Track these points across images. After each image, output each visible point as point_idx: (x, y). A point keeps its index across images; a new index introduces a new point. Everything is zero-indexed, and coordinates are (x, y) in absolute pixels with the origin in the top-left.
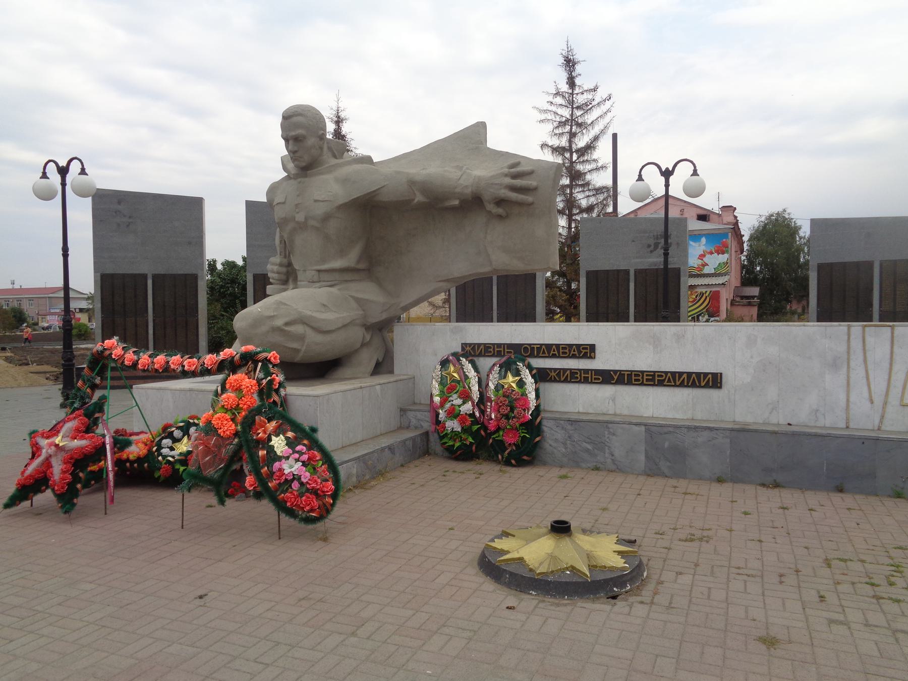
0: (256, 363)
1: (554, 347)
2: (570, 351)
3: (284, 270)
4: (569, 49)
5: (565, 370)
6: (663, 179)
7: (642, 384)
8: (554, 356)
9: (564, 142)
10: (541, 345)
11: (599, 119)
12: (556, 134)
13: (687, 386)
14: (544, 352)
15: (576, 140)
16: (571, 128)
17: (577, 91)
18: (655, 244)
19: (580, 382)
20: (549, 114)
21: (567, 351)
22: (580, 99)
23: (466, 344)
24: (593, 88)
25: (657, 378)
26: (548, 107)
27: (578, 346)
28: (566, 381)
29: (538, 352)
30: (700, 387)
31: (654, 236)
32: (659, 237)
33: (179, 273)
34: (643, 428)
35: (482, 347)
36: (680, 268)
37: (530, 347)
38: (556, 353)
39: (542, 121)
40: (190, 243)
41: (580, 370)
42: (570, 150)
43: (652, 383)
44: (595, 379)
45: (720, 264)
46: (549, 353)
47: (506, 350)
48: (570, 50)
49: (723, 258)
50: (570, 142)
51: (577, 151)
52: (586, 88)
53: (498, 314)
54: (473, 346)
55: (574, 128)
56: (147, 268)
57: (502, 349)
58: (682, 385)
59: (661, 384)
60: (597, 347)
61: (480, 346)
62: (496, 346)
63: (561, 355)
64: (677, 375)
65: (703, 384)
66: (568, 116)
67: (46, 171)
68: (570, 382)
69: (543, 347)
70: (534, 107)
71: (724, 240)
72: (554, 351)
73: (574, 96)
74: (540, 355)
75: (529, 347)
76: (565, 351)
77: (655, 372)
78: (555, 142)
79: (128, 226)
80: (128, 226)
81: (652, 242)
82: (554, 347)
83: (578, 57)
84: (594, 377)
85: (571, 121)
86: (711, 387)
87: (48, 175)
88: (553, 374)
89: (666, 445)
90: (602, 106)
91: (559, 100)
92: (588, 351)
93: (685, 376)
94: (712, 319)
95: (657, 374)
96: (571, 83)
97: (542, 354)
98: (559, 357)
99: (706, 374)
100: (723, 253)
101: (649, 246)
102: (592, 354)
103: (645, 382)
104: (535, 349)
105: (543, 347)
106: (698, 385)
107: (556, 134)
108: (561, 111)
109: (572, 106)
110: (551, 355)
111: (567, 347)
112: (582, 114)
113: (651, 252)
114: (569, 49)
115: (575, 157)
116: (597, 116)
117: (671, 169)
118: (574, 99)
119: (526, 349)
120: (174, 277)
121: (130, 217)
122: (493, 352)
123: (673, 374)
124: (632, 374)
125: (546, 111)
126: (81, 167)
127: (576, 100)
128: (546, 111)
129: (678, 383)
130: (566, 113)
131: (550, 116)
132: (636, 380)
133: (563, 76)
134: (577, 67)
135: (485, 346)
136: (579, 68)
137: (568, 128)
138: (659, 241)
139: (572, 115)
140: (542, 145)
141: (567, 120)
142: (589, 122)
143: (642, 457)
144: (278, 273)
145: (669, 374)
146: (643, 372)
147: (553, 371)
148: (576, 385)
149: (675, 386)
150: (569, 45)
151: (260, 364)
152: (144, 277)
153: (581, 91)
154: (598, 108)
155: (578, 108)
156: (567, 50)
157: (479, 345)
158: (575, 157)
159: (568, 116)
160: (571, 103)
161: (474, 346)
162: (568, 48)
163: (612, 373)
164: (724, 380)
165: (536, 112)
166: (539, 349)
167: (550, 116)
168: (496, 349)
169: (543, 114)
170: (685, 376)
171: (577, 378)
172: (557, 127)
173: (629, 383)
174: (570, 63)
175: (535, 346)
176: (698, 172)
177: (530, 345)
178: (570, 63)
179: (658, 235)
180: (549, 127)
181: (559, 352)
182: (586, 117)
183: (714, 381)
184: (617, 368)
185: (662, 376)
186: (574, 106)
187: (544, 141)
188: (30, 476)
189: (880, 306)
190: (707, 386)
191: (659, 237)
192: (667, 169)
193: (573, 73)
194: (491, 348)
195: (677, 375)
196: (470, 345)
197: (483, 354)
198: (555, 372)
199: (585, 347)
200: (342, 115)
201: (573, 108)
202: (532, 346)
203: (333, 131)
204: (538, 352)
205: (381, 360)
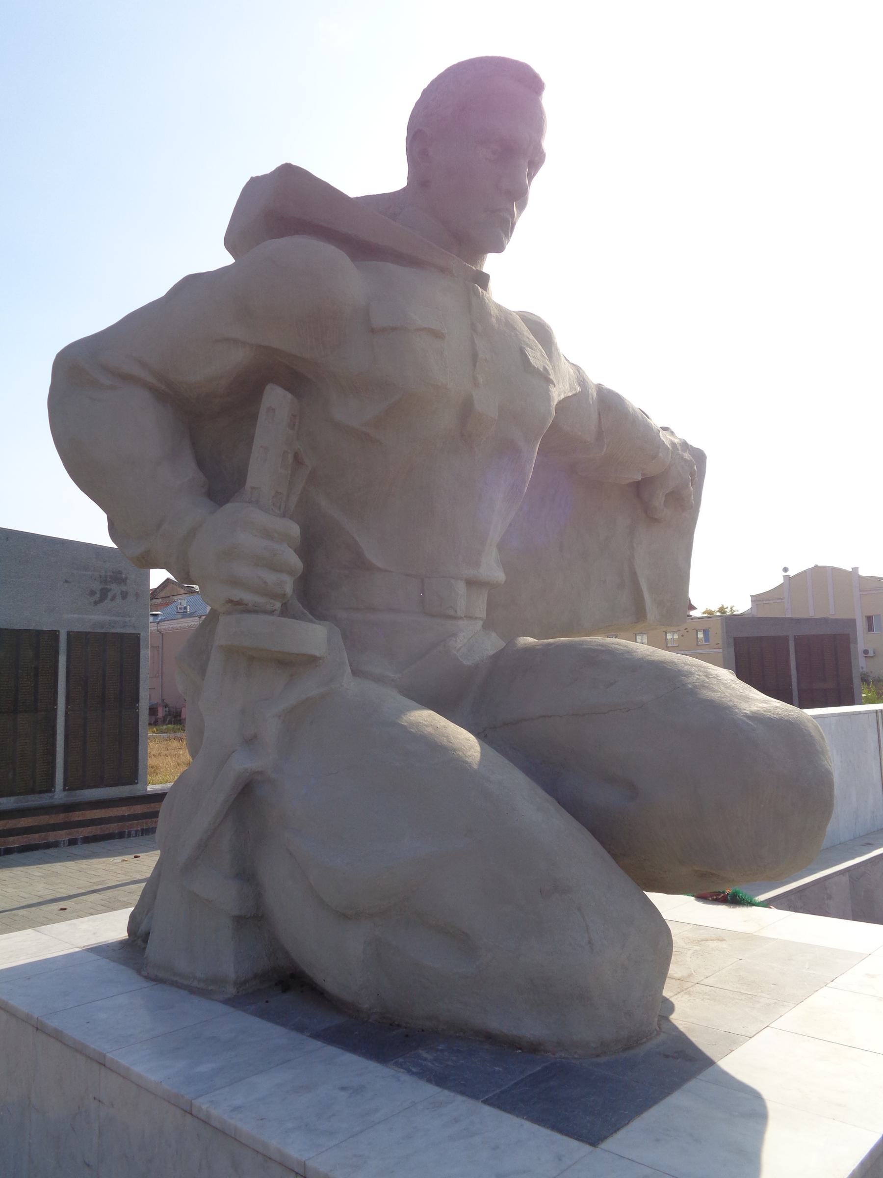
18: (102, 590)
31: (100, 576)
32: (109, 579)
36: (139, 634)
81: (97, 586)
101: (92, 593)
113: (96, 603)
138: (108, 587)
179: (106, 577)
191: (109, 579)
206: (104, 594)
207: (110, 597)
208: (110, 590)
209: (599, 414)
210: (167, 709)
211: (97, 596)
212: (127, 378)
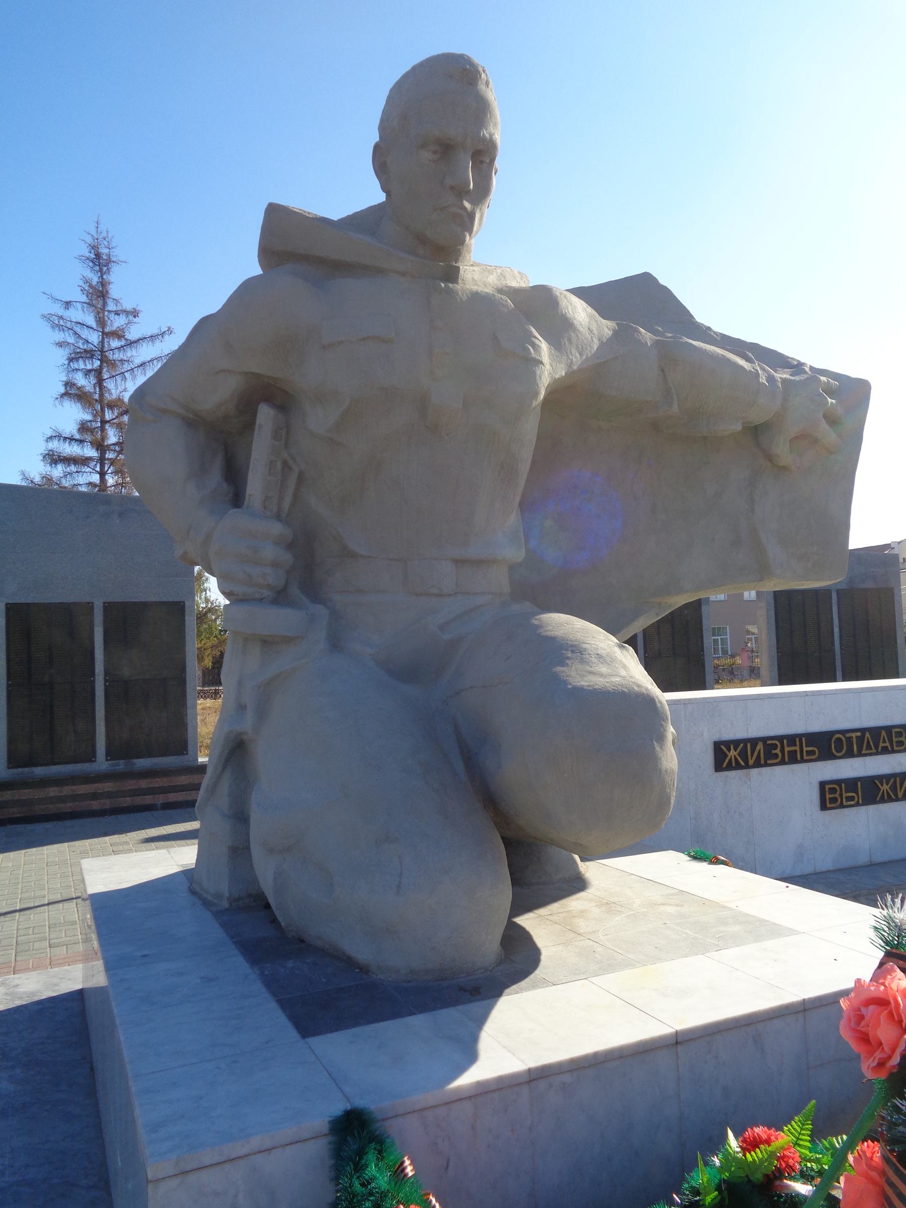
1: (883, 733)
3: (287, 558)
4: (104, 234)
8: (885, 751)
10: (863, 730)
14: (869, 747)
15: (110, 384)
16: (101, 366)
17: (111, 306)
20: (66, 333)
23: (728, 744)
35: (760, 746)
37: (844, 736)
38: (887, 744)
39: (60, 345)
46: (877, 748)
47: (805, 749)
51: (111, 406)
53: (106, 681)
54: (742, 745)
57: (797, 748)
61: (757, 744)
62: (785, 741)
63: (895, 748)
69: (868, 735)
72: (884, 742)
73: (106, 313)
74: (863, 752)
75: (843, 738)
76: (901, 739)
82: (883, 733)
83: (118, 253)
85: (101, 353)
88: (885, 787)
90: (157, 342)
97: (866, 749)
98: (893, 752)
104: (854, 741)
105: (868, 735)
108: (85, 333)
109: (103, 329)
110: (880, 750)
111: (902, 731)
112: (122, 347)
116: (153, 356)
119: (839, 739)
122: (780, 755)
130: (94, 338)
134: (115, 269)
137: (97, 363)
139: (102, 342)
142: (138, 361)
144: (275, 565)
147: (884, 780)
150: (102, 227)
157: (754, 742)
160: (101, 322)
161: (745, 746)
165: (45, 327)
166: (860, 740)
167: (71, 339)
168: (787, 749)
169: (57, 332)
175: (854, 735)
177: (843, 732)
182: (129, 354)
194: (775, 746)
196: (736, 743)
197: (762, 762)
198: (887, 784)
201: (103, 333)
202: (848, 735)
209: (663, 370)
212: (164, 411)
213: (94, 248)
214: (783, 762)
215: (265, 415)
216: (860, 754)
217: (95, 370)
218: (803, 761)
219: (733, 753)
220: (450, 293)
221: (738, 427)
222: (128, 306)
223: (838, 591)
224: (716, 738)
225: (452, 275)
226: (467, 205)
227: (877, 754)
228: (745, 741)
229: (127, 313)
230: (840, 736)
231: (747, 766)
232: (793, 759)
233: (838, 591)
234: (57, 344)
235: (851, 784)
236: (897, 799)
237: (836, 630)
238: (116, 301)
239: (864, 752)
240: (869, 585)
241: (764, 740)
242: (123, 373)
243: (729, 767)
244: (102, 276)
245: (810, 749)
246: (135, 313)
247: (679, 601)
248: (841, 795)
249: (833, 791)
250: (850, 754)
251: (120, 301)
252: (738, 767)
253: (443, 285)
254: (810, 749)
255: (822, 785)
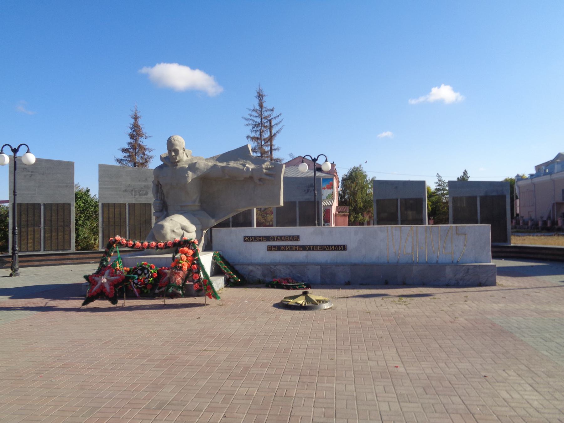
0: (190, 244)
2: (290, 238)
5: (288, 246)
6: (313, 162)
7: (318, 250)
8: (283, 240)
9: (257, 135)
10: (278, 236)
11: (276, 125)
12: (253, 131)
13: (334, 250)
14: (279, 239)
15: (263, 134)
17: (264, 110)
19: (294, 250)
20: (250, 121)
21: (288, 238)
22: (266, 114)
24: (271, 109)
25: (323, 248)
26: (249, 117)
27: (293, 236)
28: (288, 250)
29: (277, 239)
30: (339, 250)
33: (60, 202)
34: (319, 266)
35: (253, 238)
38: (284, 239)
39: (247, 125)
40: (67, 186)
41: (294, 246)
42: (261, 139)
43: (321, 250)
44: (300, 249)
45: (329, 194)
47: (263, 239)
48: (260, 89)
49: (330, 191)
50: (261, 134)
51: (264, 140)
52: (268, 109)
55: (263, 128)
56: (41, 200)
58: (332, 250)
59: (325, 250)
60: (300, 236)
64: (331, 246)
65: (340, 249)
66: (260, 122)
67: (3, 150)
68: (290, 250)
69: (279, 237)
70: (242, 118)
71: (331, 182)
73: (263, 112)
77: (322, 246)
78: (253, 135)
79: (31, 176)
80: (31, 176)
83: (264, 93)
84: (299, 248)
86: (343, 250)
87: (4, 152)
88: (283, 248)
89: (328, 272)
90: (277, 119)
91: (255, 114)
92: (297, 238)
93: (333, 247)
94: (326, 224)
95: (323, 246)
96: (261, 105)
98: (285, 241)
99: (341, 246)
100: (330, 189)
102: (298, 240)
103: (319, 249)
106: (338, 249)
107: (253, 131)
108: (256, 119)
113: (306, 193)
114: (260, 89)
115: (263, 143)
116: (275, 124)
117: (316, 158)
118: (262, 114)
120: (58, 205)
121: (32, 172)
123: (329, 246)
124: (314, 247)
125: (248, 119)
126: (27, 149)
127: (263, 114)
128: (248, 119)
129: (331, 249)
130: (259, 120)
131: (251, 122)
132: (315, 249)
133: (256, 102)
135: (254, 238)
136: (265, 99)
137: (260, 128)
139: (261, 121)
140: (247, 138)
141: (259, 124)
143: (319, 278)
145: (328, 246)
146: (318, 246)
148: (292, 252)
149: (330, 250)
150: (260, 87)
151: (191, 244)
152: (39, 205)
153: (266, 110)
154: (275, 120)
155: (264, 118)
156: (259, 89)
157: (252, 237)
158: (263, 143)
159: (260, 122)
160: (261, 116)
162: (259, 88)
163: (306, 246)
164: (347, 248)
166: (277, 238)
167: (251, 122)
168: (259, 239)
170: (333, 247)
171: (292, 249)
172: (254, 127)
173: (313, 250)
174: (260, 96)
175: (275, 237)
176: (328, 160)
177: (273, 236)
178: (260, 96)
180: (250, 127)
181: (285, 238)
183: (344, 248)
184: (308, 244)
185: (325, 247)
186: (263, 117)
187: (248, 135)
188: (95, 291)
189: (401, 218)
190: (341, 250)
192: (315, 158)
193: (262, 101)
195: (331, 246)
196: (248, 237)
198: (284, 247)
199: (296, 236)
200: (138, 115)
203: (133, 123)
204: (277, 239)
205: (206, 244)
206: (308, 191)
207: (310, 190)
208: (309, 189)
210: (533, 222)
211: (306, 191)
213: (258, 93)
214: (258, 241)
215: (159, 185)
216: (277, 241)
217: (259, 130)
218: (262, 241)
219: (247, 238)
220: (175, 168)
221: (243, 179)
222: (270, 107)
223: (481, 197)
224: (245, 235)
225: (177, 165)
226: (174, 157)
227: (281, 241)
228: (250, 237)
229: (270, 110)
230: (272, 237)
231: (250, 241)
232: (260, 240)
233: (481, 197)
234: (246, 125)
235: (274, 247)
236: (286, 250)
237: (479, 211)
238: (265, 108)
239: (278, 240)
240: (494, 194)
241: (254, 237)
242: (267, 130)
243: (246, 241)
244: (261, 101)
245: (265, 239)
246: (272, 110)
247: (242, 210)
248: (272, 248)
249: (269, 247)
250: (274, 240)
251: (267, 107)
252: (248, 241)
253: (174, 167)
254: (265, 239)
255: (268, 246)
